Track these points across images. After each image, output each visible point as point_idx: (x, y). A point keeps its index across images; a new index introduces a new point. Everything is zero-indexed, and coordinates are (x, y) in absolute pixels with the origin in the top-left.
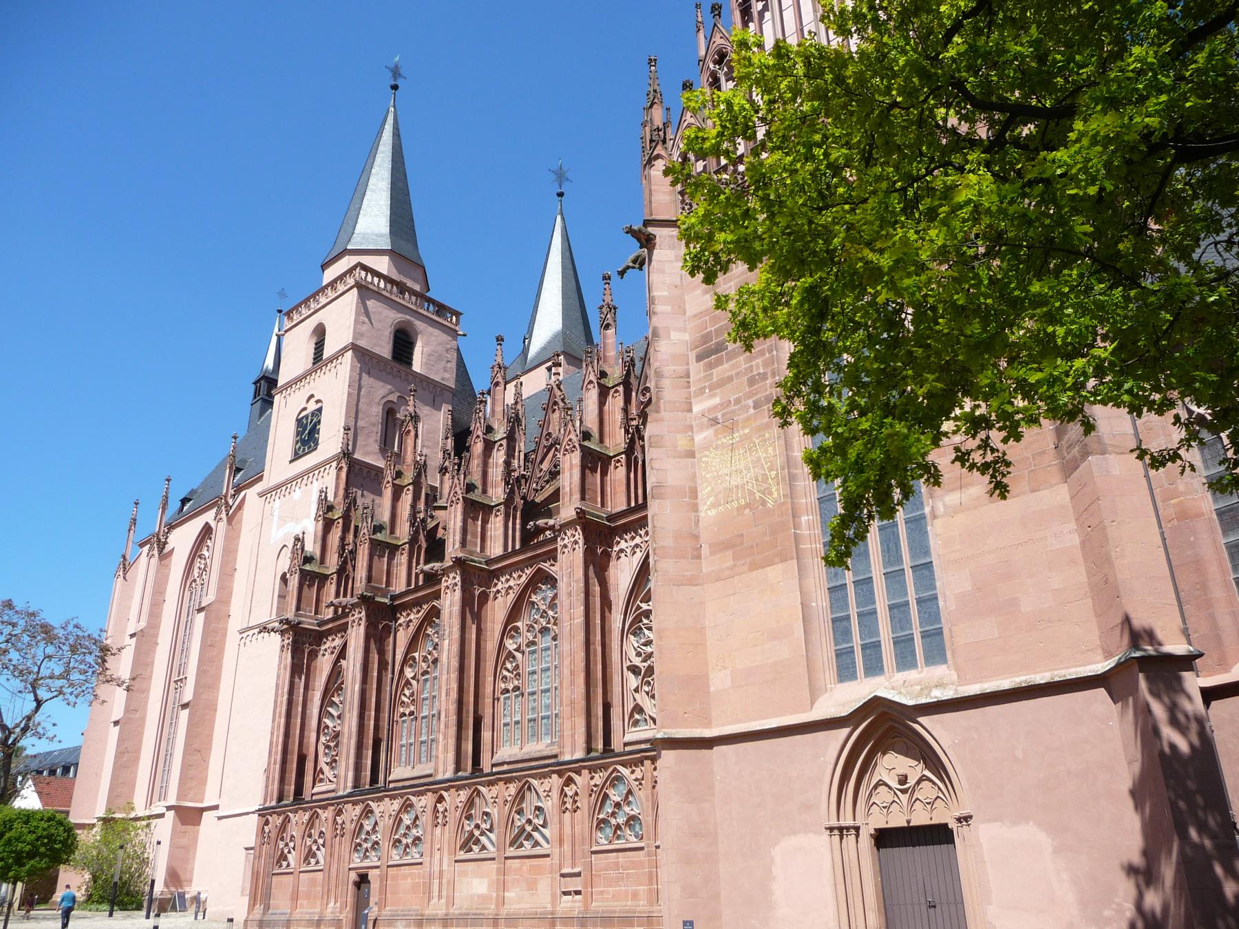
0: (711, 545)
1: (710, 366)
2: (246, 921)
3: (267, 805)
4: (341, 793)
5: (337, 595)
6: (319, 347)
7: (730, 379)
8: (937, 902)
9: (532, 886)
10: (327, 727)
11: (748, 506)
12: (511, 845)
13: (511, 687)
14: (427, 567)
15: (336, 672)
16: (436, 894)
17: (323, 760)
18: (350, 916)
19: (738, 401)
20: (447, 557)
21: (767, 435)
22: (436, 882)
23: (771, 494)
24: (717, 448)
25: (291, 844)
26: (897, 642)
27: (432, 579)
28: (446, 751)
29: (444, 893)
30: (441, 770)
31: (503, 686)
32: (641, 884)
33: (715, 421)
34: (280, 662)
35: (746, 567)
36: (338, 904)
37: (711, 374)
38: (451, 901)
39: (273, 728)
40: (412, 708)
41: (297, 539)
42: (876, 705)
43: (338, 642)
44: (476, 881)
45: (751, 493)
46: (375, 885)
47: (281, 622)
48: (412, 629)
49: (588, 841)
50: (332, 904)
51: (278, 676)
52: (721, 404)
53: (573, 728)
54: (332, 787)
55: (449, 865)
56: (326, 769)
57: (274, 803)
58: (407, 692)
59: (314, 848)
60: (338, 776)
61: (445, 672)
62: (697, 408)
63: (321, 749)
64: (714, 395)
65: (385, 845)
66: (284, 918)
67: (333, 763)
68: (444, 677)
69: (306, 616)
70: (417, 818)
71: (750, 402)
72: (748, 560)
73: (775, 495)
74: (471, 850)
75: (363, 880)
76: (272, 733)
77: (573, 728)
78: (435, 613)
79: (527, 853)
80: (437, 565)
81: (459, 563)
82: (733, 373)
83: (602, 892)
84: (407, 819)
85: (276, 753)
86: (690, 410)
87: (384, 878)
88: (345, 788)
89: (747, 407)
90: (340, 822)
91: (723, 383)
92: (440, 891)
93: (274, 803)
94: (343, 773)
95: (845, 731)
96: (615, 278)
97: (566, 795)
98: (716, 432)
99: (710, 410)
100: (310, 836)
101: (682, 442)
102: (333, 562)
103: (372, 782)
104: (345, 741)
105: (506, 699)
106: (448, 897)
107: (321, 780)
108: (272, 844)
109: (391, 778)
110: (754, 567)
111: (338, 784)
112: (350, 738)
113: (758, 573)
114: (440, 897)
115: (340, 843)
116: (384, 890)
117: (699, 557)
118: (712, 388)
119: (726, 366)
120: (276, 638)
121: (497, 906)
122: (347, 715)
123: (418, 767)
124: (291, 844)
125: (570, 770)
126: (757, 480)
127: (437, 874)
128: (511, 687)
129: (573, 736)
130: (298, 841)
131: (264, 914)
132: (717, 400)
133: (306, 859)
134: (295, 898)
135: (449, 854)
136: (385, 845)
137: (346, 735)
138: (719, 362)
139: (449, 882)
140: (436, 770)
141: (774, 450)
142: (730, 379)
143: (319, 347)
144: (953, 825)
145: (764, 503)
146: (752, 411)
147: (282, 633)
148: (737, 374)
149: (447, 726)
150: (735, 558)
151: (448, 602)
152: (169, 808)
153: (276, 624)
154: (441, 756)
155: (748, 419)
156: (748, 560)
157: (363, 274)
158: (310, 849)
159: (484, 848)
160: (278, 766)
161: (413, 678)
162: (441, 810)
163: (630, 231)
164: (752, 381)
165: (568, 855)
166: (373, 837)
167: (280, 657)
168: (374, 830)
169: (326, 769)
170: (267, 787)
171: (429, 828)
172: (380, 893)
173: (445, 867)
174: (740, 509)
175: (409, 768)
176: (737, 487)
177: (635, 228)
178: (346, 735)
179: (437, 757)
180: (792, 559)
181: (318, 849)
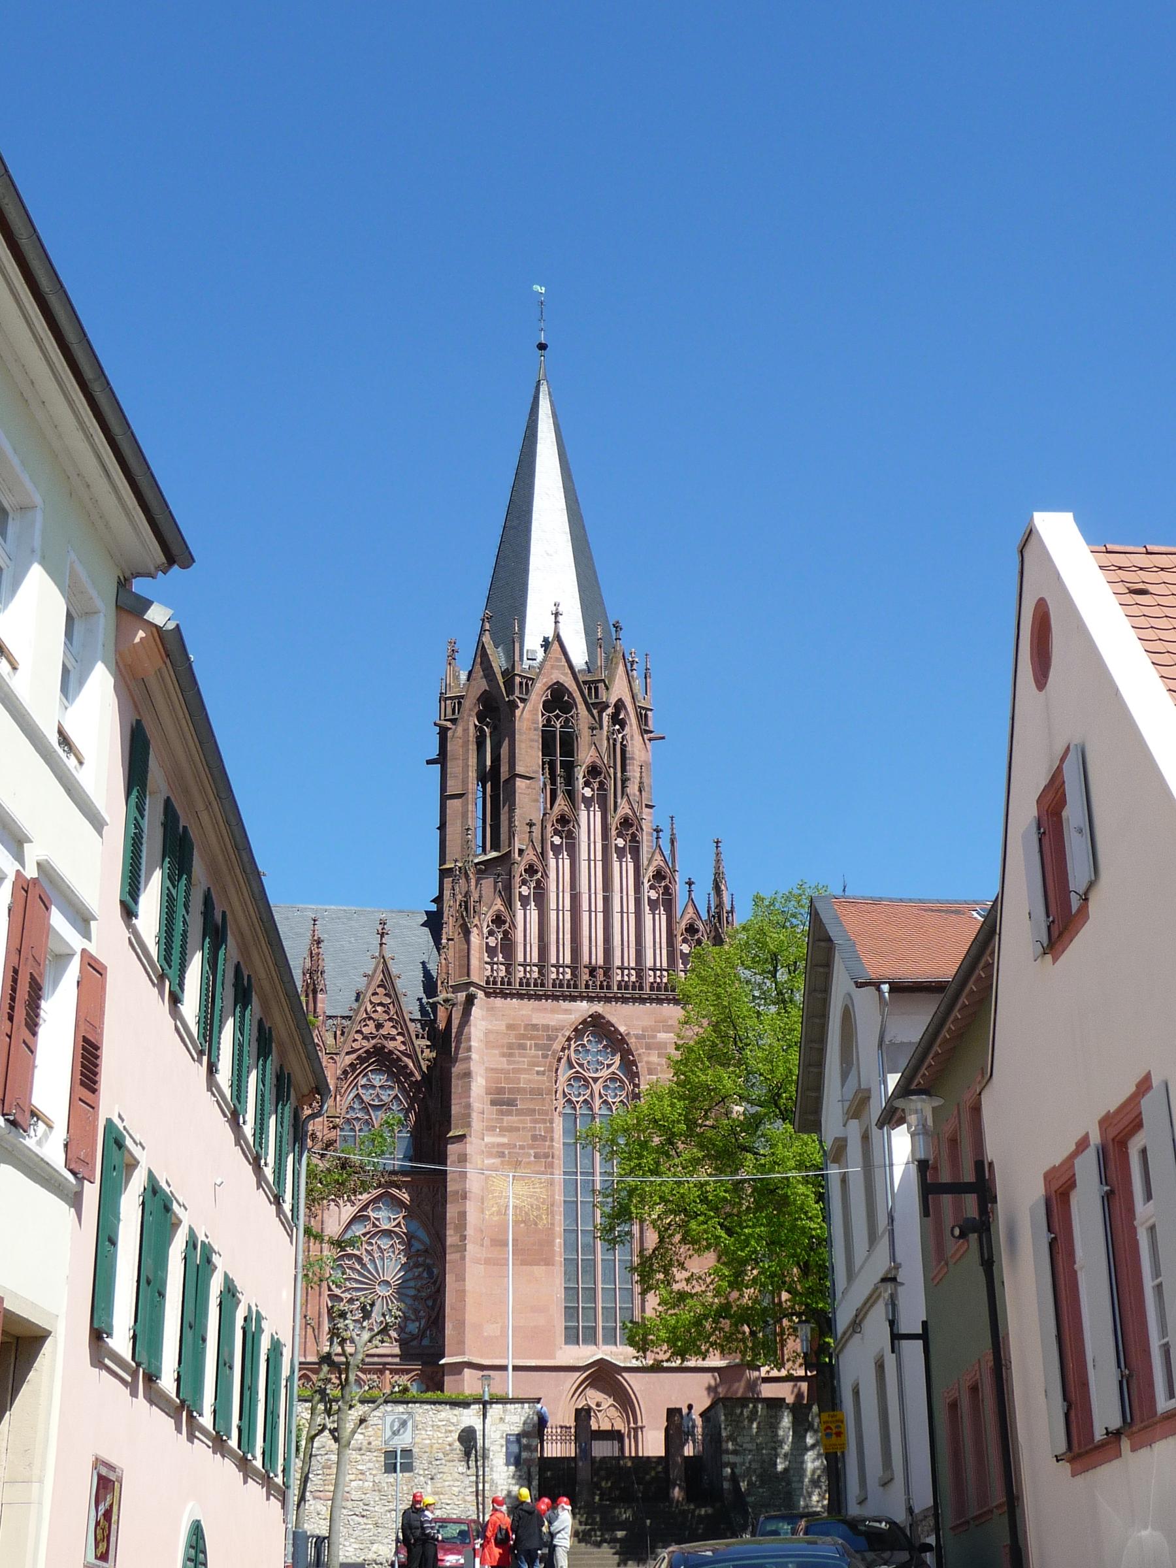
0: (492, 1240)
1: (502, 1113)
7: (517, 1129)
11: (523, 1222)
19: (522, 1147)
33: (502, 1155)
42: (601, 1362)
62: (487, 1139)
64: (500, 1135)
71: (532, 1152)
91: (512, 1129)
99: (499, 1145)
118: (502, 1129)
119: (514, 1118)
132: (505, 1140)
138: (509, 1113)
142: (517, 1129)
145: (536, 1224)
148: (524, 1128)
155: (529, 1163)
164: (534, 1138)
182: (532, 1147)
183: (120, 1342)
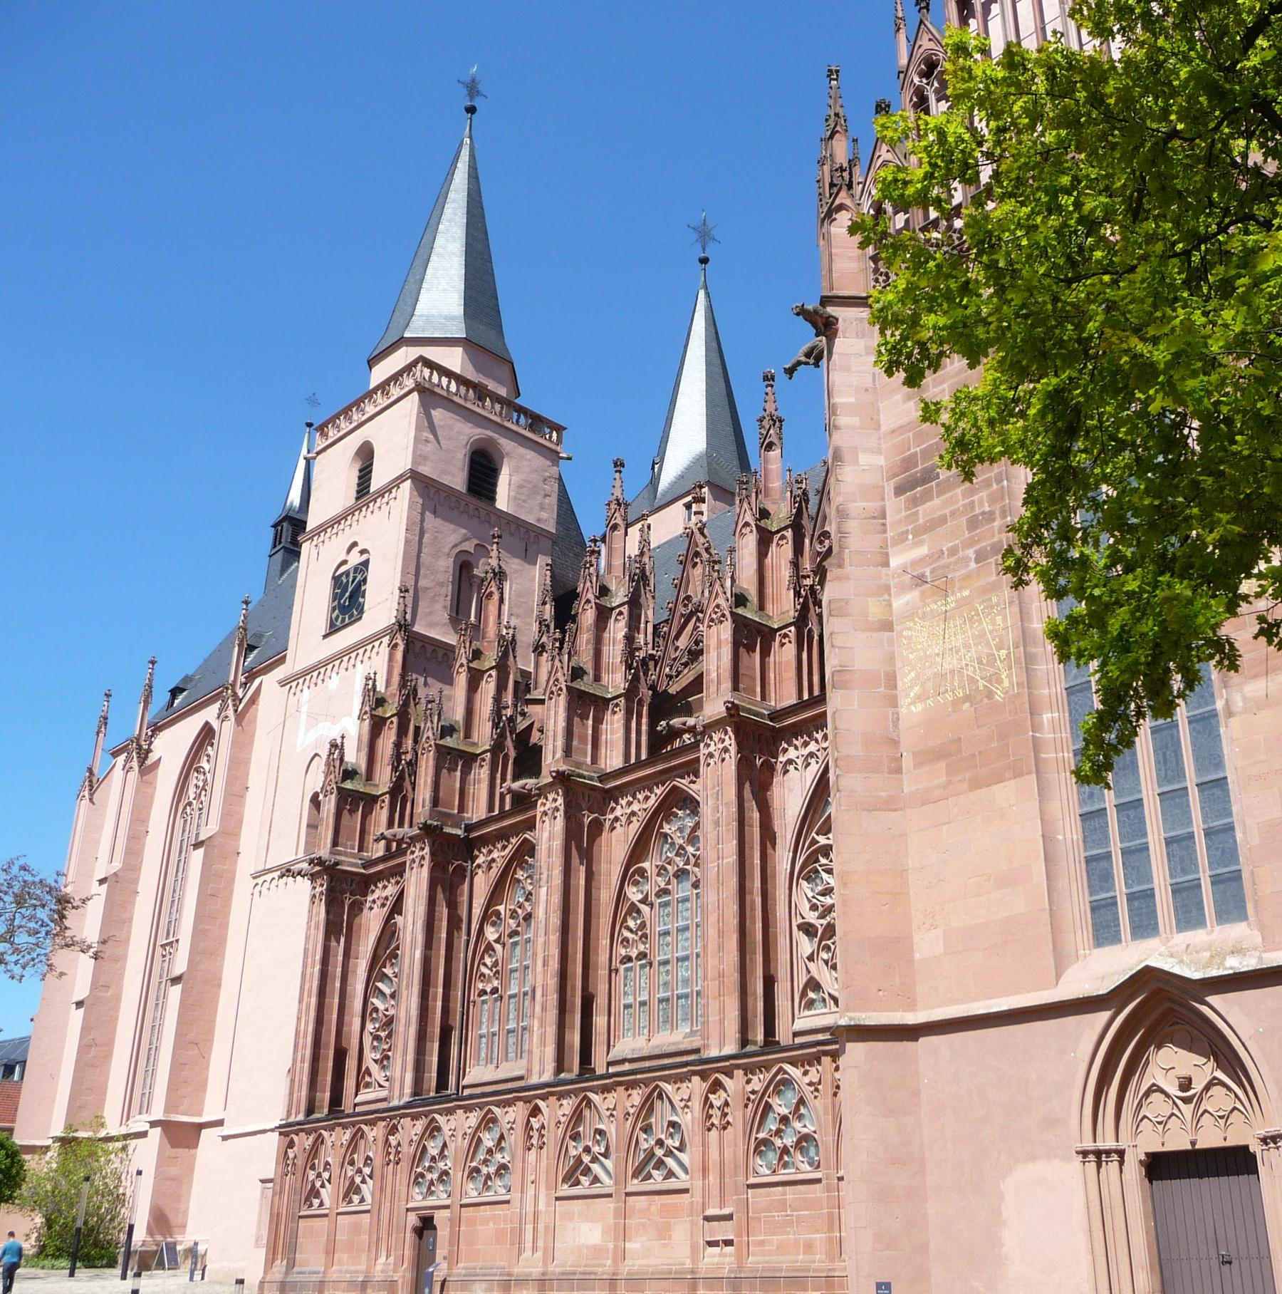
0: (916, 755)
1: (915, 502)
2: (262, 1283)
3: (292, 1119)
4: (395, 1103)
5: (390, 824)
6: (365, 475)
7: (943, 520)
8: (1234, 1256)
9: (663, 1233)
10: (376, 1010)
11: (967, 698)
12: (635, 1175)
13: (634, 954)
14: (516, 785)
15: (388, 933)
16: (529, 1244)
17: (370, 1056)
18: (408, 1275)
19: (953, 551)
20: (545, 771)
21: (994, 599)
22: (529, 1227)
23: (1000, 681)
24: (923, 617)
25: (326, 1175)
26: (1177, 890)
27: (524, 801)
28: (543, 1043)
29: (540, 1243)
30: (536, 1069)
31: (623, 952)
32: (817, 1231)
33: (921, 580)
34: (310, 919)
35: (965, 786)
36: (391, 1259)
37: (916, 514)
38: (550, 1254)
39: (300, 1011)
40: (496, 983)
41: (334, 745)
42: (1147, 978)
43: (391, 890)
44: (585, 1227)
45: (972, 681)
46: (443, 1232)
47: (311, 862)
48: (495, 872)
49: (742, 1170)
50: (382, 1259)
51: (307, 938)
52: (930, 556)
53: (722, 1011)
54: (383, 1094)
55: (548, 1205)
56: (375, 1069)
57: (301, 1117)
58: (488, 961)
59: (358, 1180)
60: (391, 1080)
61: (541, 932)
62: (895, 562)
63: (367, 1040)
64: (917, 544)
65: (457, 1176)
66: (314, 1278)
67: (384, 1061)
68: (541, 940)
69: (346, 854)
70: (502, 1137)
71: (971, 553)
72: (968, 775)
73: (1006, 683)
74: (578, 1183)
75: (426, 1225)
76: (299, 1019)
77: (722, 1011)
78: (528, 849)
79: (657, 1187)
80: (530, 782)
81: (562, 779)
82: (947, 511)
83: (762, 1243)
84: (488, 1140)
85: (304, 1047)
86: (887, 564)
87: (456, 1222)
88: (401, 1096)
89: (966, 560)
90: (394, 1143)
92: (534, 1240)
93: (301, 1117)
94: (398, 1075)
95: (1104, 1016)
96: (781, 378)
97: (712, 1106)
98: (922, 594)
99: (915, 563)
100: (352, 1163)
101: (875, 609)
102: (384, 779)
103: (438, 1088)
104: (401, 1029)
105: (627, 970)
106: (546, 1248)
107: (368, 1085)
108: (299, 1175)
109: (466, 1082)
110: (976, 784)
111: (391, 1089)
112: (408, 1025)
113: (983, 793)
114: (534, 1249)
115: (395, 1173)
116: (455, 1238)
117: (899, 771)
118: (917, 533)
119: (936, 502)
120: (304, 885)
121: (615, 1262)
122: (404, 993)
123: (504, 1065)
124: (326, 1175)
125: (718, 1070)
126: (980, 662)
127: (530, 1217)
128: (634, 954)
129: (722, 1022)
130: (335, 1170)
131: (287, 1273)
132: (923, 550)
133: (346, 1195)
134: (331, 1251)
135: (548, 1188)
136: (457, 1176)
137: (403, 1021)
138: (927, 497)
139: (547, 1228)
140: (529, 1071)
141: (1005, 620)
142: (943, 520)
143: (365, 475)
144: (1255, 1147)
145: (990, 695)
146: (973, 565)
147: (313, 877)
148: (953, 513)
149: (544, 1009)
150: (950, 771)
151: (546, 835)
152: (153, 1124)
153: (305, 865)
154: (536, 1051)
155: (968, 576)
156: (968, 775)
157: (427, 372)
158: (353, 1182)
159: (596, 1180)
160: (307, 1065)
161: (497, 941)
162: (536, 1126)
163: (802, 312)
164: (973, 524)
165: (715, 1190)
166: (441, 1165)
167: (310, 911)
168: (442, 1155)
169: (375, 1069)
170: (291, 1094)
171: (520, 1151)
172: (451, 1244)
173: (542, 1207)
174: (957, 703)
175: (491, 1067)
176: (952, 672)
177: (810, 307)
178: (403, 1021)
179: (530, 1052)
180: (1030, 773)
181: (363, 1181)
182: (969, 544)
183: (798, 1040)
